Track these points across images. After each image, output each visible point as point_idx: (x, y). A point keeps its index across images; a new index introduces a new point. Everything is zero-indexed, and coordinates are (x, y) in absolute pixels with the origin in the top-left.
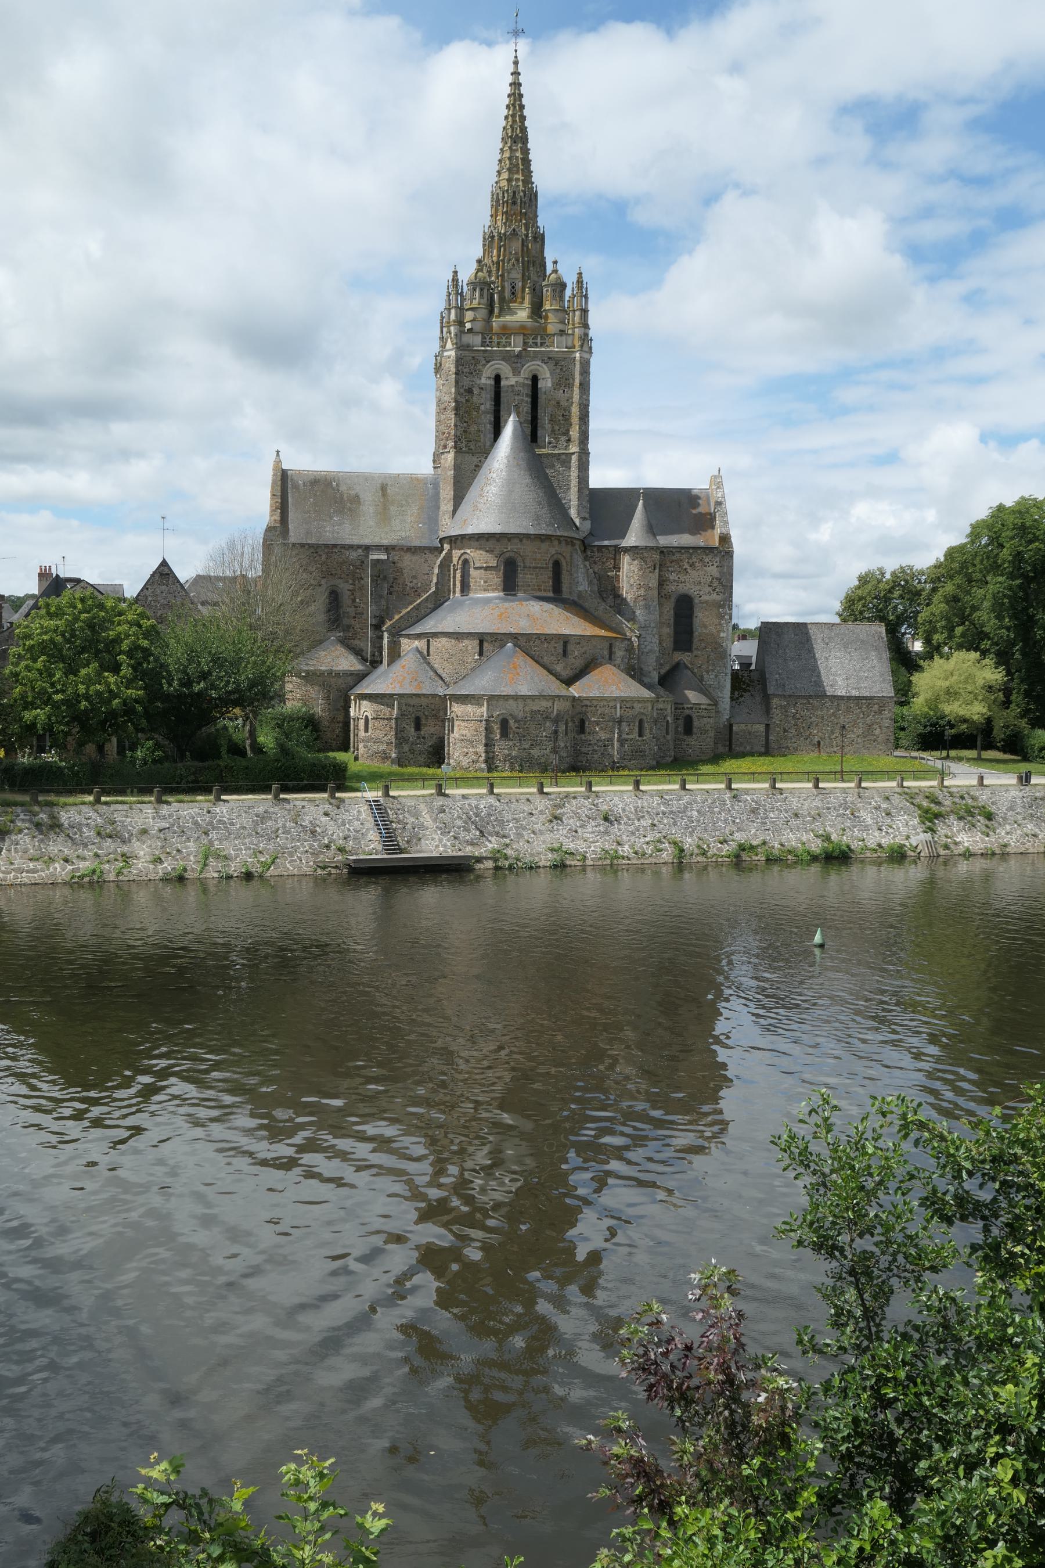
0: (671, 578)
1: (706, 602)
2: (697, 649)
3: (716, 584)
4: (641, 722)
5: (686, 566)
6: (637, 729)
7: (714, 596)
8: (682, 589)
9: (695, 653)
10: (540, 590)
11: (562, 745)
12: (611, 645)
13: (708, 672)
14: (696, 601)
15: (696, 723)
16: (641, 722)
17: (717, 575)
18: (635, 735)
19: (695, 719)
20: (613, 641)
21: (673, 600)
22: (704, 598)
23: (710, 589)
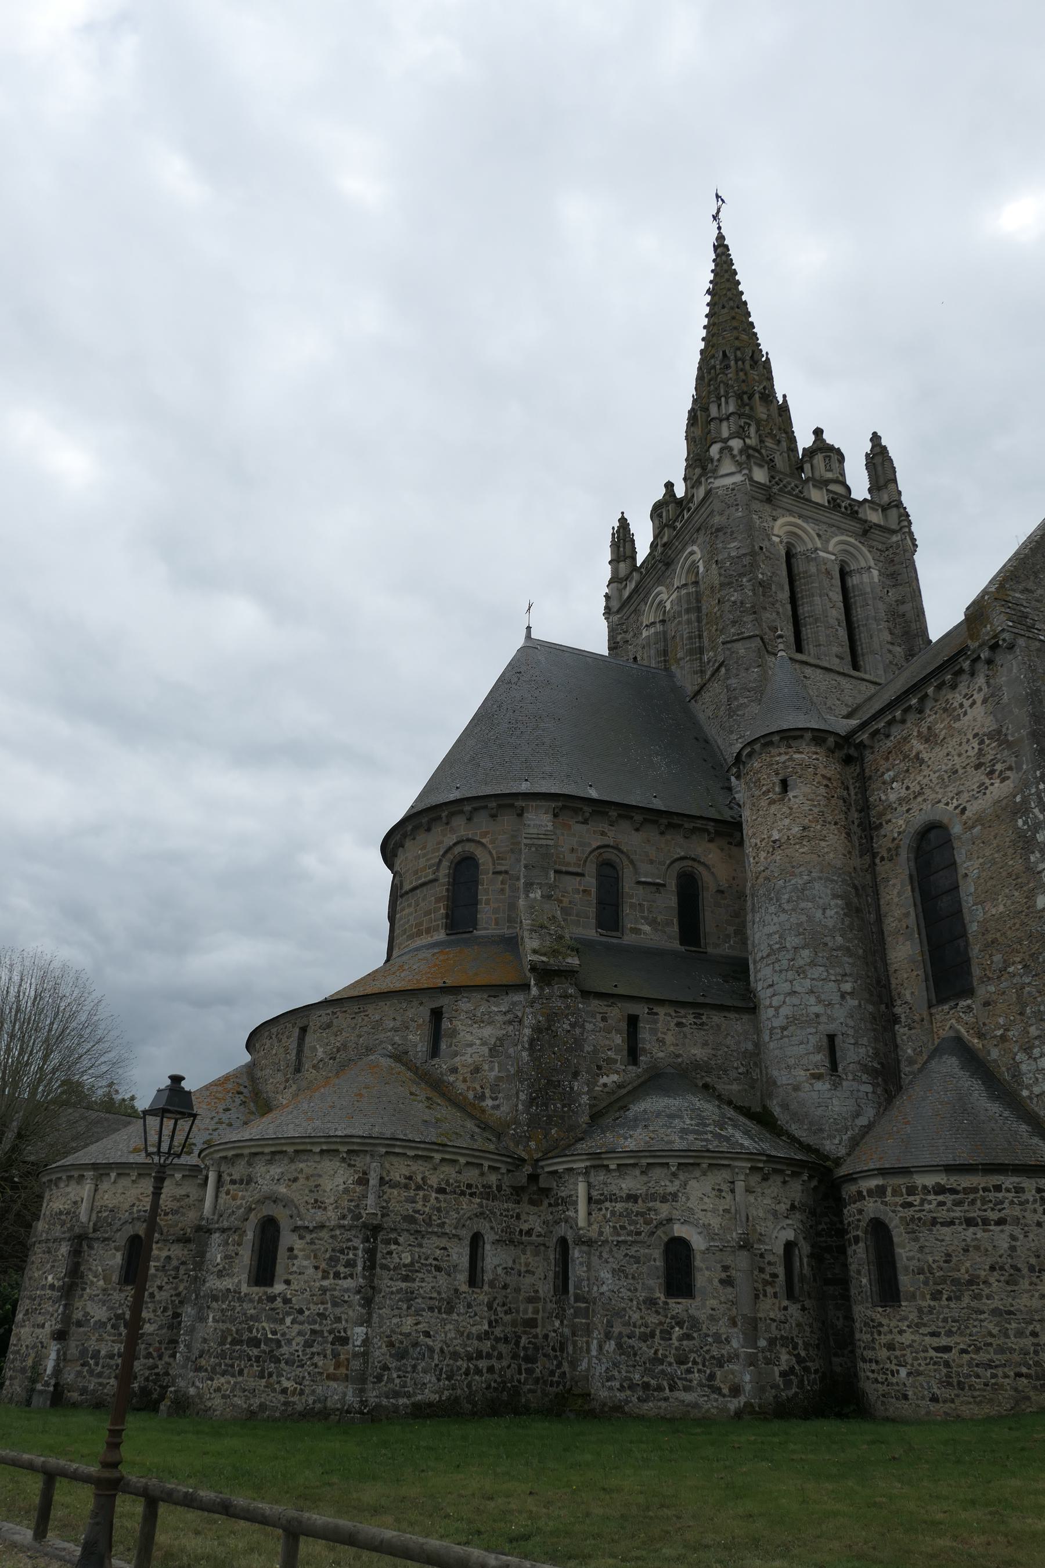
0: (893, 797)
1: (979, 820)
2: (986, 979)
3: (991, 750)
4: (269, 1229)
5: (917, 745)
6: (246, 1256)
7: (998, 790)
8: (921, 814)
9: (984, 991)
10: (419, 934)
11: (99, 1313)
12: (437, 1015)
13: (1027, 1049)
14: (956, 829)
15: (905, 1251)
16: (269, 1229)
17: (989, 724)
18: (239, 1279)
19: (899, 1234)
20: (444, 1001)
21: (904, 854)
22: (973, 809)
23: (980, 776)
